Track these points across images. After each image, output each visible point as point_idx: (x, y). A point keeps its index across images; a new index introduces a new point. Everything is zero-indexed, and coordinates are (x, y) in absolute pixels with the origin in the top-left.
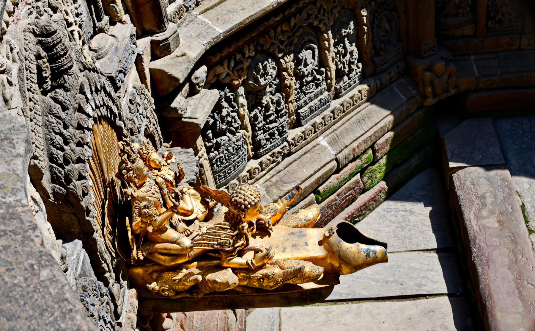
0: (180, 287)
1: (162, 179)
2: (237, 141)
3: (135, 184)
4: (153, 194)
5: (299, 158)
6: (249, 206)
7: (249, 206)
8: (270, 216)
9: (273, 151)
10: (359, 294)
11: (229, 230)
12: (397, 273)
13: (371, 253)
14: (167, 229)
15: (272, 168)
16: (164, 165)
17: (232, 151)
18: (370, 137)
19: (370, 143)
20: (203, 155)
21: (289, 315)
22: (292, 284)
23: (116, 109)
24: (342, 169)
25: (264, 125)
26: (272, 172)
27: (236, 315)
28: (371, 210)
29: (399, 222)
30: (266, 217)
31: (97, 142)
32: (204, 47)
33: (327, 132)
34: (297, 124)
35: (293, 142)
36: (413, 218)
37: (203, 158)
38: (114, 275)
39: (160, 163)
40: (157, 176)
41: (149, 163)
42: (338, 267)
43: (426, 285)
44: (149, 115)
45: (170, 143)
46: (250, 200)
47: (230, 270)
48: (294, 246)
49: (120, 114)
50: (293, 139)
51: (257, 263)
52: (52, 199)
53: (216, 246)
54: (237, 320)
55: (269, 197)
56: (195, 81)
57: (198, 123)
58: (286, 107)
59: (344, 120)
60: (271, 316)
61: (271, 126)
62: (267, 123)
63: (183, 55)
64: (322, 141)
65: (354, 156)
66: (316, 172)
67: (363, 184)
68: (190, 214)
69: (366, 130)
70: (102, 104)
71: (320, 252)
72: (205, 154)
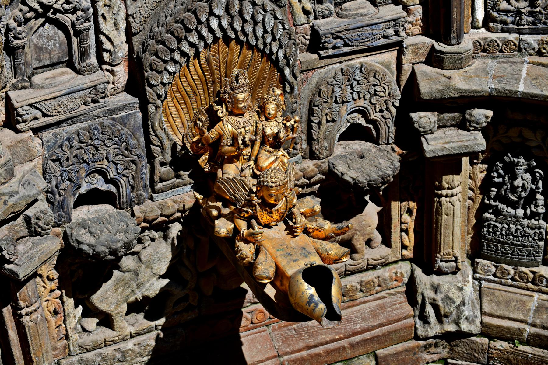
1: (261, 127)
2: (528, 226)
3: (227, 108)
4: (239, 128)
6: (262, 184)
8: (313, 227)
11: (247, 193)
13: (313, 304)
17: (513, 230)
32: (489, 90)
37: (448, 199)
38: (168, 157)
39: (269, 114)
40: (261, 121)
45: (404, 152)
47: (233, 225)
52: (135, 56)
55: (532, 316)
56: (467, 116)
63: (448, 78)
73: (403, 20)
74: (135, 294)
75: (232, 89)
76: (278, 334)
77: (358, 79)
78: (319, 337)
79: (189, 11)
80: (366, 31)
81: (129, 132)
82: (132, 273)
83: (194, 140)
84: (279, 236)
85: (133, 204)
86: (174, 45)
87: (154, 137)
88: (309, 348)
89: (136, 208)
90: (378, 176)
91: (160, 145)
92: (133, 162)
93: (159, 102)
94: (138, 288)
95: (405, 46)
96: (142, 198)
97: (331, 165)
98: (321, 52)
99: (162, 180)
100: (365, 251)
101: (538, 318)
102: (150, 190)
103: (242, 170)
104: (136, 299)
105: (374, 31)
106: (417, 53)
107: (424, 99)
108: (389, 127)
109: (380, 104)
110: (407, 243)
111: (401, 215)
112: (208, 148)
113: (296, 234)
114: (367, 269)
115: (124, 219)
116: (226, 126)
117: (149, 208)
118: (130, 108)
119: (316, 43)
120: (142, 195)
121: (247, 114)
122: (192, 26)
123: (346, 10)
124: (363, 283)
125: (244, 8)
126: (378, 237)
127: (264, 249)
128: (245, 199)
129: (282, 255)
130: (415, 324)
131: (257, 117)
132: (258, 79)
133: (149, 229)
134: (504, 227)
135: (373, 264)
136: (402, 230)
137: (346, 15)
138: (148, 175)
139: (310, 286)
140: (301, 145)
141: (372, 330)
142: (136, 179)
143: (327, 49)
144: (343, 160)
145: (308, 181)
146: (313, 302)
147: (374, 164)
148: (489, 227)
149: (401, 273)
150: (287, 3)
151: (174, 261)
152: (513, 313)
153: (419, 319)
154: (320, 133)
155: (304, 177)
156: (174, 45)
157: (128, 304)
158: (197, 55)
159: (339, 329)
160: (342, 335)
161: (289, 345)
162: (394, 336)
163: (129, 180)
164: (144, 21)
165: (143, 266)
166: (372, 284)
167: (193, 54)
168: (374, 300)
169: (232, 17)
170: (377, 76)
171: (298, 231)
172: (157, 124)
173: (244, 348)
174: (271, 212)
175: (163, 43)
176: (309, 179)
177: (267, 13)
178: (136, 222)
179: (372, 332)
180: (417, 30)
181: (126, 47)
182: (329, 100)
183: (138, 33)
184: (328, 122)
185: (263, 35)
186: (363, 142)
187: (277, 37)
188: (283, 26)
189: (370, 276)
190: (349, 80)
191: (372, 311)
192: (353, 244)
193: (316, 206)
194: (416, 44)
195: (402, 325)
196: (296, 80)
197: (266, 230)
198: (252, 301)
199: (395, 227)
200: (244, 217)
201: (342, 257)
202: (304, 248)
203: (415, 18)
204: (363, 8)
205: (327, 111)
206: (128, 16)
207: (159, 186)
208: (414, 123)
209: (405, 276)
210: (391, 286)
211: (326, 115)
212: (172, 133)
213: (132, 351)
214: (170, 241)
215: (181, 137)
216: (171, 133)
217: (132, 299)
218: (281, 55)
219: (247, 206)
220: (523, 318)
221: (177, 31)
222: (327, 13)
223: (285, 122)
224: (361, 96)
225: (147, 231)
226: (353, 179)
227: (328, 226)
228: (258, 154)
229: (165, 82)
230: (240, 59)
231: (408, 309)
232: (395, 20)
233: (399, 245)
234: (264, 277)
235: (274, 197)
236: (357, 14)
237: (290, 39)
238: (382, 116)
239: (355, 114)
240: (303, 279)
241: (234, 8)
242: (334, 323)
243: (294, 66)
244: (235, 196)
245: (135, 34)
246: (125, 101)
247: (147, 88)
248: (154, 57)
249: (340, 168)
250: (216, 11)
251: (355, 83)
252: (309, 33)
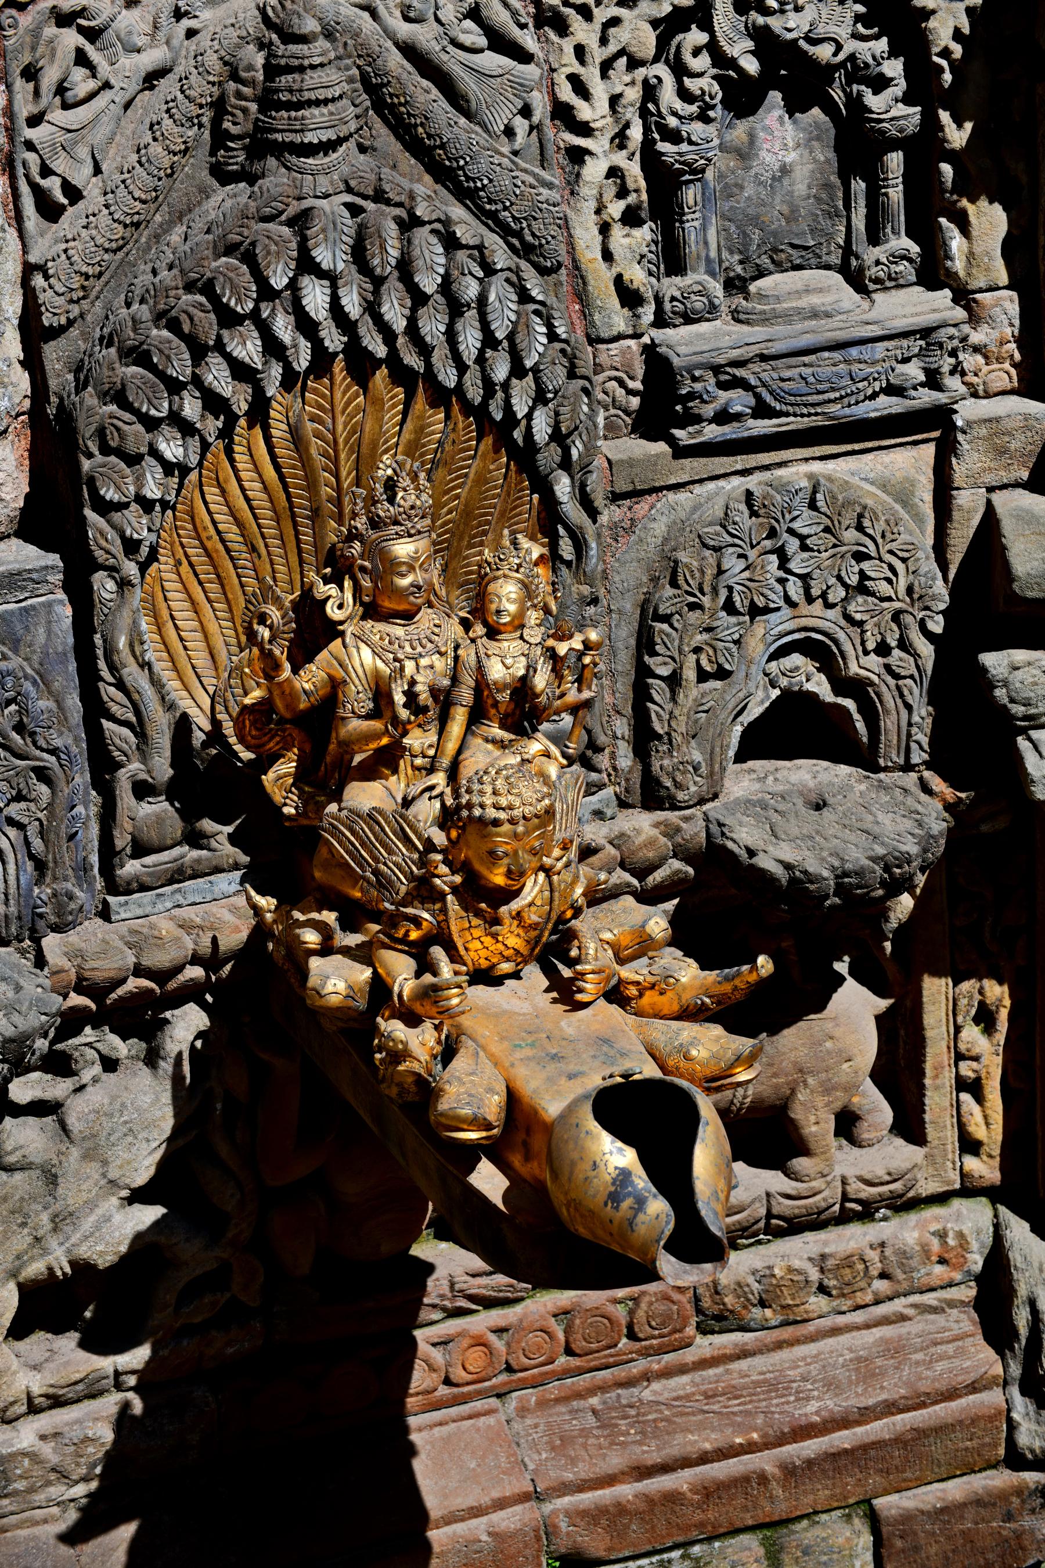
1: (473, 658)
4: (396, 660)
6: (465, 813)
8: (640, 978)
11: (416, 856)
38: (163, 769)
39: (498, 612)
40: (473, 641)
45: (963, 795)
46: (476, 799)
47: (368, 973)
52: (51, 411)
57: (1030, 769)
73: (952, 331)
74: (46, 1252)
75: (375, 523)
76: (536, 1426)
77: (805, 531)
78: (679, 1438)
79: (230, 250)
80: (827, 365)
81: (29, 671)
82: (35, 1173)
83: (247, 701)
84: (525, 1007)
85: (41, 924)
86: (181, 367)
87: (112, 690)
88: (644, 1472)
89: (51, 942)
90: (874, 859)
91: (134, 719)
92: (43, 774)
93: (131, 568)
94: (55, 1230)
95: (959, 423)
96: (73, 906)
97: (714, 829)
98: (678, 433)
99: (140, 849)
100: (839, 1155)
102: (99, 884)
103: (407, 803)
104: (50, 1269)
105: (855, 367)
106: (1001, 452)
107: (1026, 600)
108: (909, 707)
109: (878, 625)
110: (978, 1130)
111: (958, 1029)
112: (295, 733)
113: (579, 997)
114: (844, 1218)
115: (8, 973)
116: (354, 651)
117: (99, 945)
118: (31, 586)
119: (662, 403)
120: (71, 897)
121: (426, 618)
122: (239, 300)
123: (761, 296)
124: (830, 1263)
125: (416, 252)
126: (878, 1110)
127: (470, 1043)
128: (411, 877)
129: (529, 1059)
130: (1009, 1411)
131: (460, 629)
132: (467, 514)
133: (96, 1020)
135: (863, 1195)
136: (962, 1085)
137: (764, 312)
138: (94, 830)
139: (620, 1144)
140: (613, 756)
141: (859, 1423)
142: (52, 836)
143: (698, 419)
144: (756, 816)
145: (635, 882)
146: (629, 1194)
147: (859, 825)
149: (960, 1235)
150: (565, 258)
151: (181, 1142)
153: (1023, 1393)
154: (676, 712)
155: (623, 865)
156: (181, 367)
157: (20, 1286)
158: (259, 411)
159: (747, 1413)
160: (755, 1436)
161: (573, 1461)
162: (936, 1449)
163: (26, 837)
164: (83, 287)
165: (75, 1153)
166: (860, 1267)
167: (245, 407)
168: (867, 1326)
169: (378, 282)
170: (866, 523)
171: (588, 986)
172: (122, 642)
173: (418, 1465)
174: (497, 921)
175: (140, 356)
176: (641, 873)
177: (494, 278)
178: (47, 983)
179: (859, 1430)
180: (1003, 376)
181: (23, 381)
182: (706, 601)
183: (62, 330)
184: (703, 676)
185: (481, 352)
186: (825, 764)
187: (529, 363)
188: (550, 326)
189: (853, 1238)
190: (772, 534)
191: (859, 1359)
192: (792, 1121)
193: (652, 922)
194: (998, 420)
195: (963, 1409)
196: (595, 522)
197: (480, 993)
198: (447, 1303)
199: (938, 1068)
200: (404, 940)
201: (732, 1066)
202: (606, 1041)
203: (995, 334)
204: (821, 290)
205: (700, 638)
206: (29, 270)
207: (131, 868)
208: (990, 685)
209: (974, 1245)
210: (925, 1280)
211: (697, 650)
212: (176, 684)
213: (33, 1456)
214: (166, 1066)
215: (206, 703)
216: (173, 685)
217: (35, 1269)
218: (541, 427)
219: (414, 898)
221: (191, 319)
222: (699, 306)
223: (551, 642)
224: (815, 592)
225: (88, 1030)
226: (788, 866)
227: (688, 973)
228: (459, 751)
229: (149, 495)
230: (406, 436)
231: (984, 1358)
232: (926, 332)
233: (952, 1136)
234: (463, 1120)
235: (506, 861)
236: (799, 311)
237: (572, 375)
238: (888, 667)
239: (796, 659)
240: (597, 1118)
241: (383, 248)
242: (702, 1271)
243: (586, 468)
244: (376, 872)
245: (55, 333)
246: (16, 561)
247: (88, 513)
248: (113, 408)
249: (745, 834)
250: (323, 256)
251: (793, 545)
252: (640, 371)
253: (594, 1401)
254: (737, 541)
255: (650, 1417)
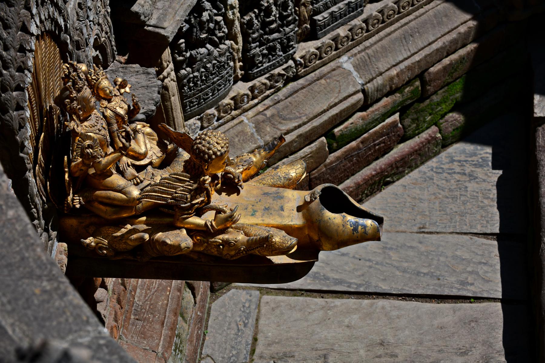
0: (122, 246)
1: (111, 112)
3: (78, 117)
4: (100, 130)
5: (309, 85)
6: (214, 157)
7: (214, 157)
8: (242, 170)
9: (272, 72)
10: (375, 287)
12: (435, 262)
13: (360, 228)
14: (112, 174)
15: (268, 97)
16: (115, 95)
17: (211, 69)
18: (418, 61)
19: (417, 71)
20: (169, 74)
21: (273, 305)
22: (259, 256)
23: (62, 20)
24: (371, 105)
25: (261, 36)
26: (267, 102)
27: (195, 297)
28: (412, 168)
29: (450, 190)
30: (237, 171)
31: (37, 62)
33: (355, 50)
34: (311, 35)
35: (302, 61)
36: (472, 186)
37: (169, 79)
39: (111, 92)
40: (106, 107)
41: (97, 91)
42: (318, 241)
43: (472, 284)
44: (101, 22)
47: (184, 231)
48: (267, 209)
49: (66, 26)
50: (302, 57)
51: (217, 226)
53: (170, 201)
54: (195, 303)
55: (259, 138)
57: (166, 35)
58: (296, 11)
59: (382, 34)
60: (247, 305)
61: (272, 37)
62: (266, 33)
64: (346, 62)
65: (391, 87)
66: (331, 107)
67: (404, 127)
68: (142, 158)
69: (412, 52)
70: (47, 17)
71: (296, 220)
72: (173, 73)
76: (132, 337)
101: (266, 135)
134: (202, 72)
148: (189, 82)
152: (244, 149)
161: (152, 337)
220: (255, 145)
253: (132, 317)
254: (83, 22)
255: (147, 308)
